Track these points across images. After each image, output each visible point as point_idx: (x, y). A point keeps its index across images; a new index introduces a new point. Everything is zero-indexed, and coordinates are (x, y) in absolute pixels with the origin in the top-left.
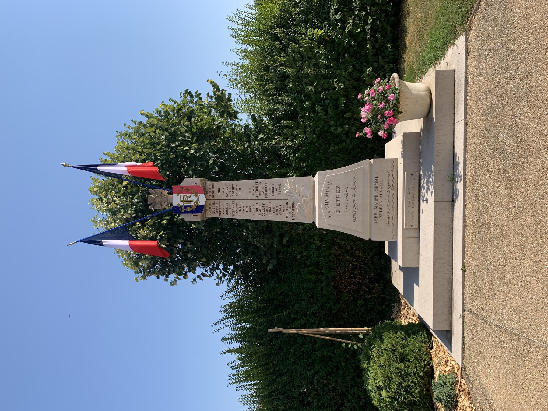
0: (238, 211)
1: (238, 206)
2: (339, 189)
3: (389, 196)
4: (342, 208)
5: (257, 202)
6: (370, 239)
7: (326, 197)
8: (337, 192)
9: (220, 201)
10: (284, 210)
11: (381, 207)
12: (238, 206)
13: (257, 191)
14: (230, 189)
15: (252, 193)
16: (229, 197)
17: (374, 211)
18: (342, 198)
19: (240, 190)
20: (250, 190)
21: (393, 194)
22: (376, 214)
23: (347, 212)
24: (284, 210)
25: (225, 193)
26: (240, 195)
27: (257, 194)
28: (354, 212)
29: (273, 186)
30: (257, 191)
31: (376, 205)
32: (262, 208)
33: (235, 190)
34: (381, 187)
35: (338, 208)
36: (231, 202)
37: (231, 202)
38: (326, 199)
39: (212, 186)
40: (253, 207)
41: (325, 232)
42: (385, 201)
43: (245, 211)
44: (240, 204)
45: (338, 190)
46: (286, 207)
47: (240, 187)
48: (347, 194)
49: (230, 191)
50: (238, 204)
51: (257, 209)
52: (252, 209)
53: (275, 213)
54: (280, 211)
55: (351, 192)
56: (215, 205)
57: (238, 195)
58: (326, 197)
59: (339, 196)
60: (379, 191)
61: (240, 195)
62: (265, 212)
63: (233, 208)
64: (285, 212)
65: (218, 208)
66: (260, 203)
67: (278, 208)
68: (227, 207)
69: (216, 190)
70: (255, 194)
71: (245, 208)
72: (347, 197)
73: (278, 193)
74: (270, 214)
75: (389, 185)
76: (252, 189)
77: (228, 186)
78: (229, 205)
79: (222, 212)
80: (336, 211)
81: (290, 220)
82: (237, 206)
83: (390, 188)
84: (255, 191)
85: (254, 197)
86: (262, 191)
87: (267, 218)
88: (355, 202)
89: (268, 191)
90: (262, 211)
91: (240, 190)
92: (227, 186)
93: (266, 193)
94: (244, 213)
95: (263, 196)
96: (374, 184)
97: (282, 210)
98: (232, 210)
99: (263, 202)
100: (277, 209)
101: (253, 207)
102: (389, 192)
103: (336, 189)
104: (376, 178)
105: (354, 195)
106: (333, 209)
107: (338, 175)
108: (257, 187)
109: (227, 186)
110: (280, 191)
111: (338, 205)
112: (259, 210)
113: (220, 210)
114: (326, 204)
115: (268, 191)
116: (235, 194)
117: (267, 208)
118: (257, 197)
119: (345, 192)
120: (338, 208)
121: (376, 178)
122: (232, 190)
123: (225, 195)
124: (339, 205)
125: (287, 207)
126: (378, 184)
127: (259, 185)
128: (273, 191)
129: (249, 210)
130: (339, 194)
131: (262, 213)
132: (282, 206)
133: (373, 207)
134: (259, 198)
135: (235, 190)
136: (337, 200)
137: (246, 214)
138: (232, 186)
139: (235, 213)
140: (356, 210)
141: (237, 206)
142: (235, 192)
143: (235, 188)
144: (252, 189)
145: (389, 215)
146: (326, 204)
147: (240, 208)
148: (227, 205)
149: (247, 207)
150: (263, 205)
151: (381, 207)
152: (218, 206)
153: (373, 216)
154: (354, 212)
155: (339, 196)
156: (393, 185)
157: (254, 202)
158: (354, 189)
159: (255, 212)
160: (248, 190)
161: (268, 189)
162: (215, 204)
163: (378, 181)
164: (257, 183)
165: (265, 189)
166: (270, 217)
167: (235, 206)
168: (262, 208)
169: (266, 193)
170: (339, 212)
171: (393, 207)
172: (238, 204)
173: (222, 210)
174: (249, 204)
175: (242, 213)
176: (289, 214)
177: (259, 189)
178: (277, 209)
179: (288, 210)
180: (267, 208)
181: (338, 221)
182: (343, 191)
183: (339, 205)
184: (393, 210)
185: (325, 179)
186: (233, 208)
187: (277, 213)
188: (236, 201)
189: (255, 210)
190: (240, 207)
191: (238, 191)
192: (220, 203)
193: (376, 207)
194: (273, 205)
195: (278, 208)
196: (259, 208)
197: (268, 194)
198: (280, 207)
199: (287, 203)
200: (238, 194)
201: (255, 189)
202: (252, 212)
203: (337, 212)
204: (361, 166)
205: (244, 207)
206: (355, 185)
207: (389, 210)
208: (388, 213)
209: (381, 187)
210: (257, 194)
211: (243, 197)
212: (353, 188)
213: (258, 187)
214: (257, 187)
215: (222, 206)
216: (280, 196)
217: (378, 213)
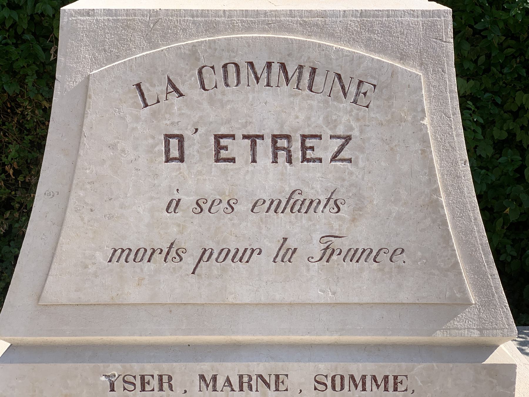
7: (276, 68)
8: (309, 143)
31: (221, 381)
38: (260, 67)
41: (52, 58)
58: (276, 68)
59: (282, 155)
80: (181, 138)
103: (327, 132)
107: (425, 152)
111: (219, 148)
114: (232, 69)
119: (309, 194)
124: (223, 154)
130: (297, 154)
140: (190, 261)
146: (232, 69)
155: (282, 155)
170: (175, 153)
181: (113, 147)
183: (223, 154)
185: (403, 57)
203: (174, 142)
204: (478, 292)
212: (336, 243)
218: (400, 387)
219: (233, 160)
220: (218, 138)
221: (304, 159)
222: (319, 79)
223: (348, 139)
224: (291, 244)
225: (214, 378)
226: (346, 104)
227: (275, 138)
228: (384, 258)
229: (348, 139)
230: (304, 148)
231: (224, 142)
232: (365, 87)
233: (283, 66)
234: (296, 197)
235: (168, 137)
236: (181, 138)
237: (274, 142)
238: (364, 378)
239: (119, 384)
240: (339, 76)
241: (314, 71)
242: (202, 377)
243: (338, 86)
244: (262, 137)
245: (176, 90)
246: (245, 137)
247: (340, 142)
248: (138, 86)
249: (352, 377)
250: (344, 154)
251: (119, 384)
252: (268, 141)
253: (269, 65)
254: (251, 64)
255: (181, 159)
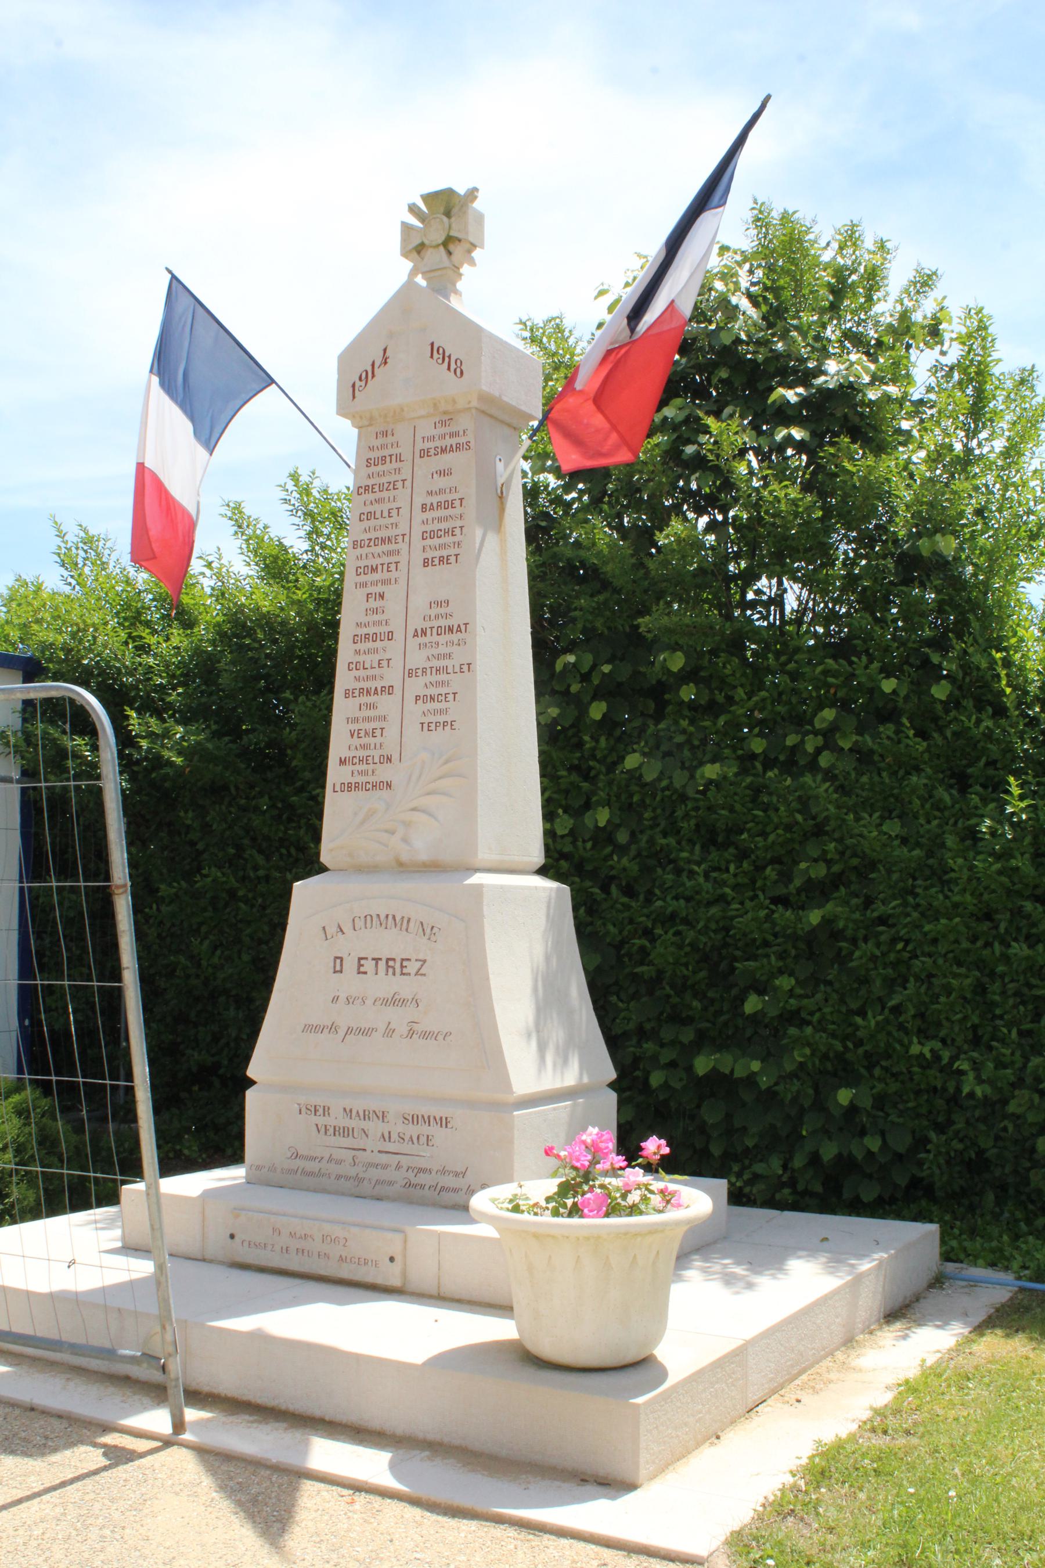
0: (374, 562)
1: (386, 560)
2: (413, 972)
3: (385, 1167)
4: (349, 983)
5: (399, 635)
6: (251, 1083)
7: (390, 917)
9: (408, 483)
10: (364, 747)
11: (346, 1132)
12: (386, 560)
13: (435, 631)
14: (446, 519)
15: (428, 612)
16: (419, 516)
17: (336, 1111)
18: (382, 984)
19: (441, 560)
20: (439, 604)
21: (391, 1183)
22: (326, 1110)
23: (335, 999)
24: (364, 747)
25: (435, 500)
26: (426, 563)
27: (424, 633)
28: (333, 1028)
29: (450, 697)
30: (435, 631)
32: (376, 658)
33: (441, 541)
34: (415, 1141)
35: (350, 965)
36: (403, 528)
37: (403, 528)
38: (383, 917)
39: (462, 440)
40: (380, 623)
42: (369, 1151)
43: (370, 590)
44: (393, 567)
45: (412, 967)
46: (376, 753)
47: (452, 559)
48: (394, 1001)
49: (440, 520)
50: (393, 559)
51: (375, 638)
52: (376, 618)
53: (358, 714)
54: (362, 734)
55: (399, 1017)
56: (394, 465)
57: (426, 555)
58: (390, 917)
59: (391, 970)
60: (400, 1128)
61: (426, 563)
62: (362, 673)
63: (383, 541)
64: (362, 753)
65: (384, 480)
66: (393, 650)
67: (373, 725)
68: (385, 514)
69: (447, 459)
70: (428, 624)
71: (379, 589)
72: (386, 1002)
73: (426, 720)
74: (357, 693)
75: (421, 1170)
76: (442, 611)
77: (458, 511)
78: (392, 520)
79: (371, 497)
80: (341, 959)
81: (335, 774)
82: (390, 553)
83: (411, 1175)
84: (436, 624)
85: (416, 623)
86: (435, 652)
87: (343, 679)
88: (366, 1032)
89: (435, 678)
90: (368, 659)
91: (441, 560)
92: (457, 503)
93: (429, 671)
94: (364, 585)
95: (417, 659)
96: (424, 1110)
97: (365, 740)
98: (373, 535)
99: (397, 663)
100: (368, 719)
101: (380, 623)
102: (398, 1167)
103: (413, 957)
104: (444, 1122)
105: (389, 1032)
106: (352, 946)
108: (451, 630)
109: (457, 503)
110: (433, 726)
111: (360, 965)
112: (370, 645)
113: (377, 489)
114: (369, 918)
115: (435, 678)
116: (429, 542)
117: (374, 678)
118: (416, 635)
120: (350, 965)
121: (444, 1122)
122: (443, 526)
123: (429, 500)
124: (362, 969)
125: (377, 760)
126: (424, 1129)
127: (455, 637)
128: (432, 698)
129: (373, 604)
131: (361, 658)
132: (378, 740)
133: (348, 1103)
134: (413, 643)
135: (441, 541)
136: (377, 960)
137: (361, 593)
138: (459, 523)
139: (366, 550)
140: (342, 1033)
141: (390, 553)
142: (436, 541)
143: (449, 539)
144: (442, 611)
145: (324, 1161)
146: (369, 918)
147: (380, 567)
148: (394, 513)
149: (382, 596)
150: (384, 663)
151: (346, 1132)
152: (392, 479)
153: (319, 1101)
154: (333, 1028)
155: (391, 970)
156: (422, 1187)
157: (396, 625)
158: (411, 1033)
159: (365, 631)
160: (441, 597)
161: (443, 677)
162: (399, 465)
163: (434, 1130)
164: (463, 628)
165: (442, 663)
166: (347, 694)
167: (386, 547)
168: (376, 658)
169: (429, 671)
170: (338, 968)
171: (348, 1178)
172: (393, 559)
173: (378, 495)
174: (393, 606)
175: (363, 578)
176: (351, 768)
177: (442, 639)
178: (368, 719)
179: (364, 767)
180: (374, 678)
182: (404, 986)
183: (362, 969)
184: (339, 1177)
186: (383, 541)
187: (356, 720)
188: (403, 547)
189: (371, 630)
190: (385, 567)
191: (437, 554)
192: (399, 485)
193: (348, 1112)
194: (387, 705)
195: (373, 725)
196: (378, 644)
197: (422, 680)
198: (378, 733)
199: (389, 759)
200: (430, 554)
201: (442, 622)
202: (364, 619)
203: (338, 961)
205: (384, 582)
206: (426, 1035)
207: (339, 1162)
208: (330, 1160)
209: (415, 1141)
210: (424, 633)
211: (420, 576)
212: (415, 1027)
213: (448, 637)
214: (451, 630)
215: (392, 493)
216: (412, 730)
217: (330, 1121)
218: (449, 1125)
219: (365, 973)
220: (360, 959)
221: (402, 974)
222: (411, 924)
223: (425, 961)
224: (392, 1026)
225: (351, 1111)
226: (424, 940)
227: (388, 960)
228: (440, 1037)
229: (425, 961)
230: (402, 967)
231: (362, 962)
232: (435, 930)
233: (394, 917)
234: (396, 997)
235: (336, 958)
236: (341, 959)
237: (387, 962)
238: (429, 1117)
239: (304, 1110)
240: (422, 923)
241: (409, 920)
242: (345, 1109)
243: (421, 930)
244: (380, 959)
245: (341, 931)
246: (373, 959)
247: (420, 963)
248: (324, 928)
249: (423, 1117)
250: (421, 972)
251: (304, 1110)
252: (384, 961)
253: (387, 916)
254: (378, 915)
255: (341, 972)
